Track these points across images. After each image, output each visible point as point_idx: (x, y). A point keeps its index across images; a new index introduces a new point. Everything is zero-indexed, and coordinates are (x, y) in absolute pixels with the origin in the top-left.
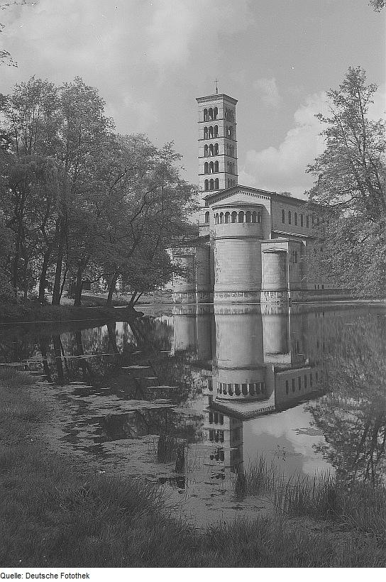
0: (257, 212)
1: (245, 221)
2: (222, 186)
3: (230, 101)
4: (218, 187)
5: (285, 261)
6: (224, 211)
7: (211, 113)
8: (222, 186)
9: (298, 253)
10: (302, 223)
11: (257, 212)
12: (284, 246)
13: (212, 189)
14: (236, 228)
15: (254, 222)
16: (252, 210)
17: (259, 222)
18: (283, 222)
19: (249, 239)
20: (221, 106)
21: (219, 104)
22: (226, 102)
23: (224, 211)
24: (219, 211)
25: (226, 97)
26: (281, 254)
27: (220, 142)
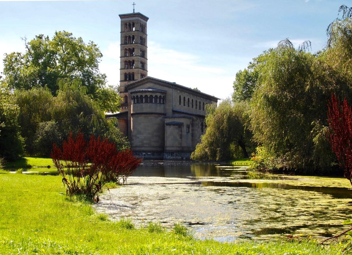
0: (162, 96)
5: (181, 131)
9: (190, 126)
10: (192, 106)
11: (162, 96)
13: (130, 80)
15: (160, 103)
16: (159, 95)
17: (163, 103)
18: (180, 104)
19: (156, 116)
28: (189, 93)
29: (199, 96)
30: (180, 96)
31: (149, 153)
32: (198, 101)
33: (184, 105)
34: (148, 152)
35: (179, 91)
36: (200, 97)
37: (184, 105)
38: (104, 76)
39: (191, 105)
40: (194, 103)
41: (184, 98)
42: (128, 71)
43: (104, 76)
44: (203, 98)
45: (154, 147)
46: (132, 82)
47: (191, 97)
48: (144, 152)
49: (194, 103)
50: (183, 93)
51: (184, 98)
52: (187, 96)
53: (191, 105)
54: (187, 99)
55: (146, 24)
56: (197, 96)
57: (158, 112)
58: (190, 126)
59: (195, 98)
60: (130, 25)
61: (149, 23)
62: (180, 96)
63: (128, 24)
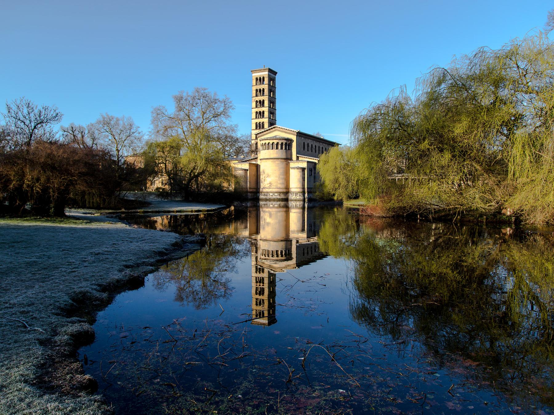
0: (288, 143)
1: (280, 148)
2: (266, 126)
3: (272, 73)
4: (263, 127)
6: (267, 142)
7: (260, 80)
8: (266, 126)
9: (313, 169)
12: (305, 165)
14: (273, 153)
20: (267, 76)
21: (265, 74)
22: (270, 74)
23: (267, 142)
24: (264, 142)
25: (270, 71)
26: (303, 169)
27: (266, 99)
28: (312, 140)
29: (321, 142)
30: (304, 143)
31: (276, 194)
32: (321, 147)
33: (308, 151)
34: (275, 193)
35: (303, 138)
36: (323, 143)
37: (308, 151)
38: (236, 126)
39: (314, 150)
40: (317, 148)
41: (308, 144)
42: (258, 121)
43: (236, 126)
44: (326, 144)
45: (280, 188)
46: (263, 130)
47: (315, 144)
48: (271, 192)
49: (317, 148)
50: (307, 139)
51: (308, 144)
52: (310, 142)
53: (314, 150)
54: (310, 145)
55: (275, 78)
56: (319, 142)
57: (272, 157)
58: (313, 169)
59: (317, 144)
60: (260, 78)
61: (277, 77)
62: (304, 143)
63: (258, 78)
